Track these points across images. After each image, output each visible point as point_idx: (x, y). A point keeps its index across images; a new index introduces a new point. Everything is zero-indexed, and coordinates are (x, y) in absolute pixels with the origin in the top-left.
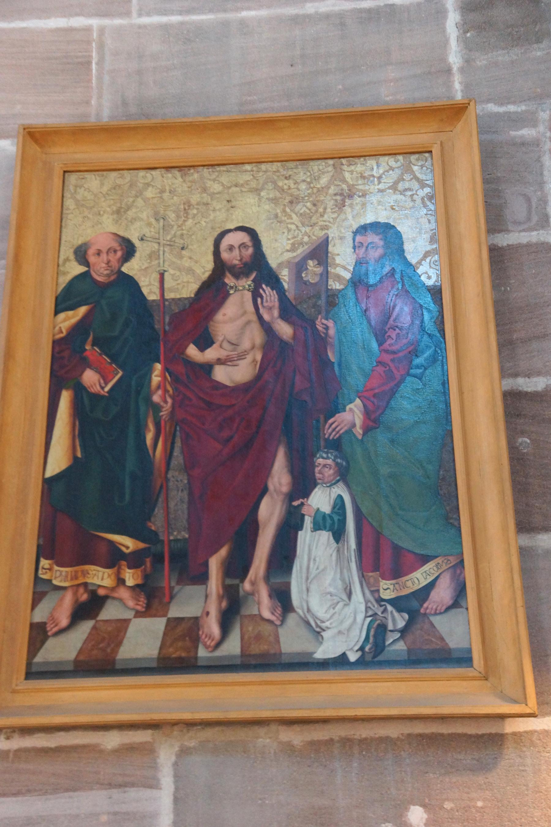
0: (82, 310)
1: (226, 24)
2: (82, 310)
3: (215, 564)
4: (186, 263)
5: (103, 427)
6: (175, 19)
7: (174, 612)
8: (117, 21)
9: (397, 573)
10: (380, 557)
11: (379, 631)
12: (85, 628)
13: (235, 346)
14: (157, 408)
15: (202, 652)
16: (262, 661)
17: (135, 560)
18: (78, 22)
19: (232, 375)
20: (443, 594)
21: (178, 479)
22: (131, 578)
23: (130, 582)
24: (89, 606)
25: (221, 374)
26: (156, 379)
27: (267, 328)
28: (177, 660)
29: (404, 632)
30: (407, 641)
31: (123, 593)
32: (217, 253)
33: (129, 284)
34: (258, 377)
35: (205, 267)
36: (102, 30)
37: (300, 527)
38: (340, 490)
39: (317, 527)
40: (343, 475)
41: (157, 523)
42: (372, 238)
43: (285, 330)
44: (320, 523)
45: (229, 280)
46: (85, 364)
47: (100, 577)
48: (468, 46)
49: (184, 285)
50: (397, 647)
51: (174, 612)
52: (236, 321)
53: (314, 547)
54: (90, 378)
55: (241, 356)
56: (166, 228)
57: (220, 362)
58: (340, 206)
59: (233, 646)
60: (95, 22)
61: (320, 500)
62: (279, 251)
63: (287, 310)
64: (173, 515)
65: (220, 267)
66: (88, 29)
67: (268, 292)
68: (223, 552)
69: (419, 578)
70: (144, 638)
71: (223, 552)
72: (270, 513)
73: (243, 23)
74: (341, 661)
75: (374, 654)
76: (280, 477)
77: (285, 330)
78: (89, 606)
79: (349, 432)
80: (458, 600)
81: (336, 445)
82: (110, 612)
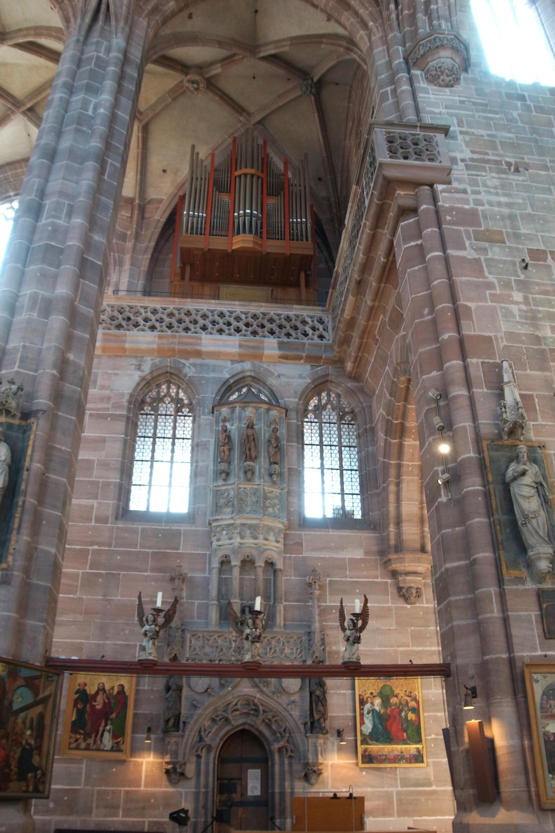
3: (93, 735)
5: (80, 713)
10: (115, 736)
11: (113, 747)
13: (99, 704)
16: (98, 750)
17: (83, 734)
19: (99, 707)
24: (77, 740)
28: (87, 748)
30: (116, 748)
33: (85, 691)
40: (112, 724)
43: (106, 701)
47: (78, 736)
50: (115, 749)
53: (106, 734)
54: (79, 706)
59: (94, 747)
60: (84, 641)
61: (108, 728)
62: (107, 687)
63: (107, 698)
64: (88, 727)
65: (99, 689)
69: (119, 740)
70: (83, 745)
72: (101, 729)
74: (107, 751)
75: (112, 750)
76: (103, 724)
77: (106, 701)
78: (77, 740)
80: (123, 743)
82: (79, 741)
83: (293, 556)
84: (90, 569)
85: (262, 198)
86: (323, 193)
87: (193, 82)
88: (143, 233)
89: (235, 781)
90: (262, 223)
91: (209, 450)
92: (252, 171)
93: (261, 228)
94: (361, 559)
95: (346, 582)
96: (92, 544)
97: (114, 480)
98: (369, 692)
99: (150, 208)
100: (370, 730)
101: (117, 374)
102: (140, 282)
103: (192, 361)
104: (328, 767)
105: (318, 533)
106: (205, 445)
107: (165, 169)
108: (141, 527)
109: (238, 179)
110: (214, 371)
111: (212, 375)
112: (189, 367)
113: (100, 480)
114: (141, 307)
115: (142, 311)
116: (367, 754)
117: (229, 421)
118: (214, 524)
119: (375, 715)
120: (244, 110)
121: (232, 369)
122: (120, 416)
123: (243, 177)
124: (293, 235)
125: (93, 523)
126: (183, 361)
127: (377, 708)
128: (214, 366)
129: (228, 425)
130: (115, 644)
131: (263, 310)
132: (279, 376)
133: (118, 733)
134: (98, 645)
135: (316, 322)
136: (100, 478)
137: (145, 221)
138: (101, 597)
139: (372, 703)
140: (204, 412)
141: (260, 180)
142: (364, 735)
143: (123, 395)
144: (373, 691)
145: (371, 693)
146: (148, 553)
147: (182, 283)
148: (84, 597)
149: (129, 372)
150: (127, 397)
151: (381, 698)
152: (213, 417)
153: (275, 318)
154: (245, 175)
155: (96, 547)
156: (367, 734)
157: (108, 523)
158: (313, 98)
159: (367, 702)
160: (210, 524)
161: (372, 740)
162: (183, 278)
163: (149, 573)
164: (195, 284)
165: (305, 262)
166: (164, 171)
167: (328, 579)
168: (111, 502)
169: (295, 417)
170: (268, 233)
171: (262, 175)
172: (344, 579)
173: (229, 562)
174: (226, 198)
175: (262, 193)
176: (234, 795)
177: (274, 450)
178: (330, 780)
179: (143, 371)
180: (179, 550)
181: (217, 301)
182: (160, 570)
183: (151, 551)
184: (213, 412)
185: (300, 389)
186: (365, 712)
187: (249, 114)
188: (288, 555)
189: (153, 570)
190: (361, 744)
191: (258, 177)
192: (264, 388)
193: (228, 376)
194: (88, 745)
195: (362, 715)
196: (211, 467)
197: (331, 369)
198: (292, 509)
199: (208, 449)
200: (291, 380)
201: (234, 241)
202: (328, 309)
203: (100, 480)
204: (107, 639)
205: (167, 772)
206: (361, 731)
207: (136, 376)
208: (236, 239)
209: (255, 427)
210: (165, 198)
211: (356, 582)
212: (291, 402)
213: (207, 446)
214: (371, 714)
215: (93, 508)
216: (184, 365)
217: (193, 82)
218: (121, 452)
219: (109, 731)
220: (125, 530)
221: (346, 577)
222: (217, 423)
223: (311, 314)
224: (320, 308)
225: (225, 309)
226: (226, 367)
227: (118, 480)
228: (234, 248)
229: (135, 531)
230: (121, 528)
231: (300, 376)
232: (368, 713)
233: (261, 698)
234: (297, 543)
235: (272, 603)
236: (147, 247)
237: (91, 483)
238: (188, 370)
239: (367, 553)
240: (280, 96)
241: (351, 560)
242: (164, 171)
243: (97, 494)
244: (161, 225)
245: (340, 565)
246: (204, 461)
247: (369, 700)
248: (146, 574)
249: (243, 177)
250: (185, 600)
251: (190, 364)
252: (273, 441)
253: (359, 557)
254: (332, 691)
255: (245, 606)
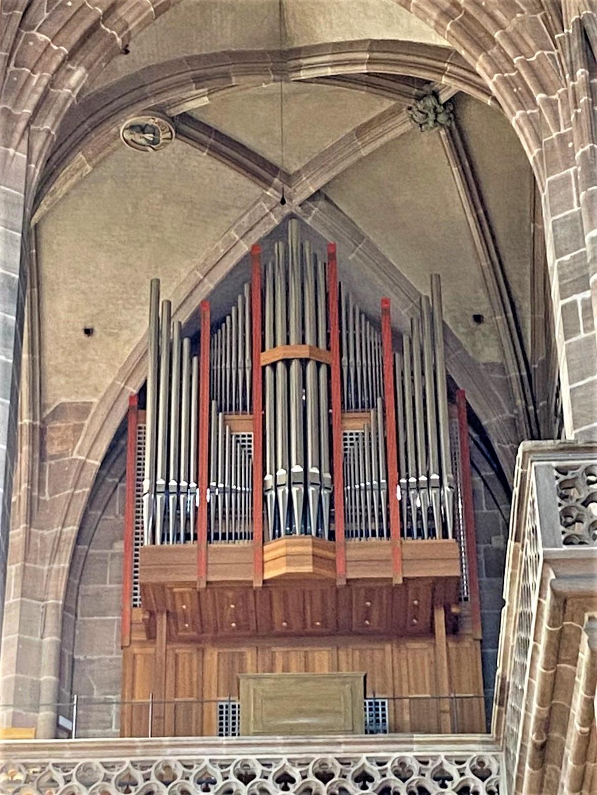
85: (330, 416)
86: (490, 354)
87: (142, 129)
88: (47, 497)
90: (332, 496)
92: (304, 352)
93: (332, 506)
99: (58, 430)
102: (47, 639)
107: (89, 326)
109: (268, 369)
114: (55, 765)
115: (59, 776)
120: (275, 170)
123: (280, 366)
124: (409, 518)
131: (342, 751)
135: (469, 775)
137: (48, 463)
141: (323, 370)
147: (150, 650)
153: (373, 770)
154: (287, 362)
158: (443, 133)
162: (151, 634)
164: (184, 651)
165: (444, 592)
166: (88, 332)
170: (347, 520)
171: (325, 357)
174: (244, 426)
175: (330, 406)
181: (234, 740)
187: (288, 178)
191: (318, 365)
201: (267, 557)
202: (498, 740)
208: (275, 549)
210: (95, 400)
217: (142, 129)
223: (457, 751)
224: (478, 737)
225: (253, 758)
228: (267, 576)
236: (59, 539)
240: (360, 131)
242: (88, 332)
244: (89, 476)
249: (280, 366)
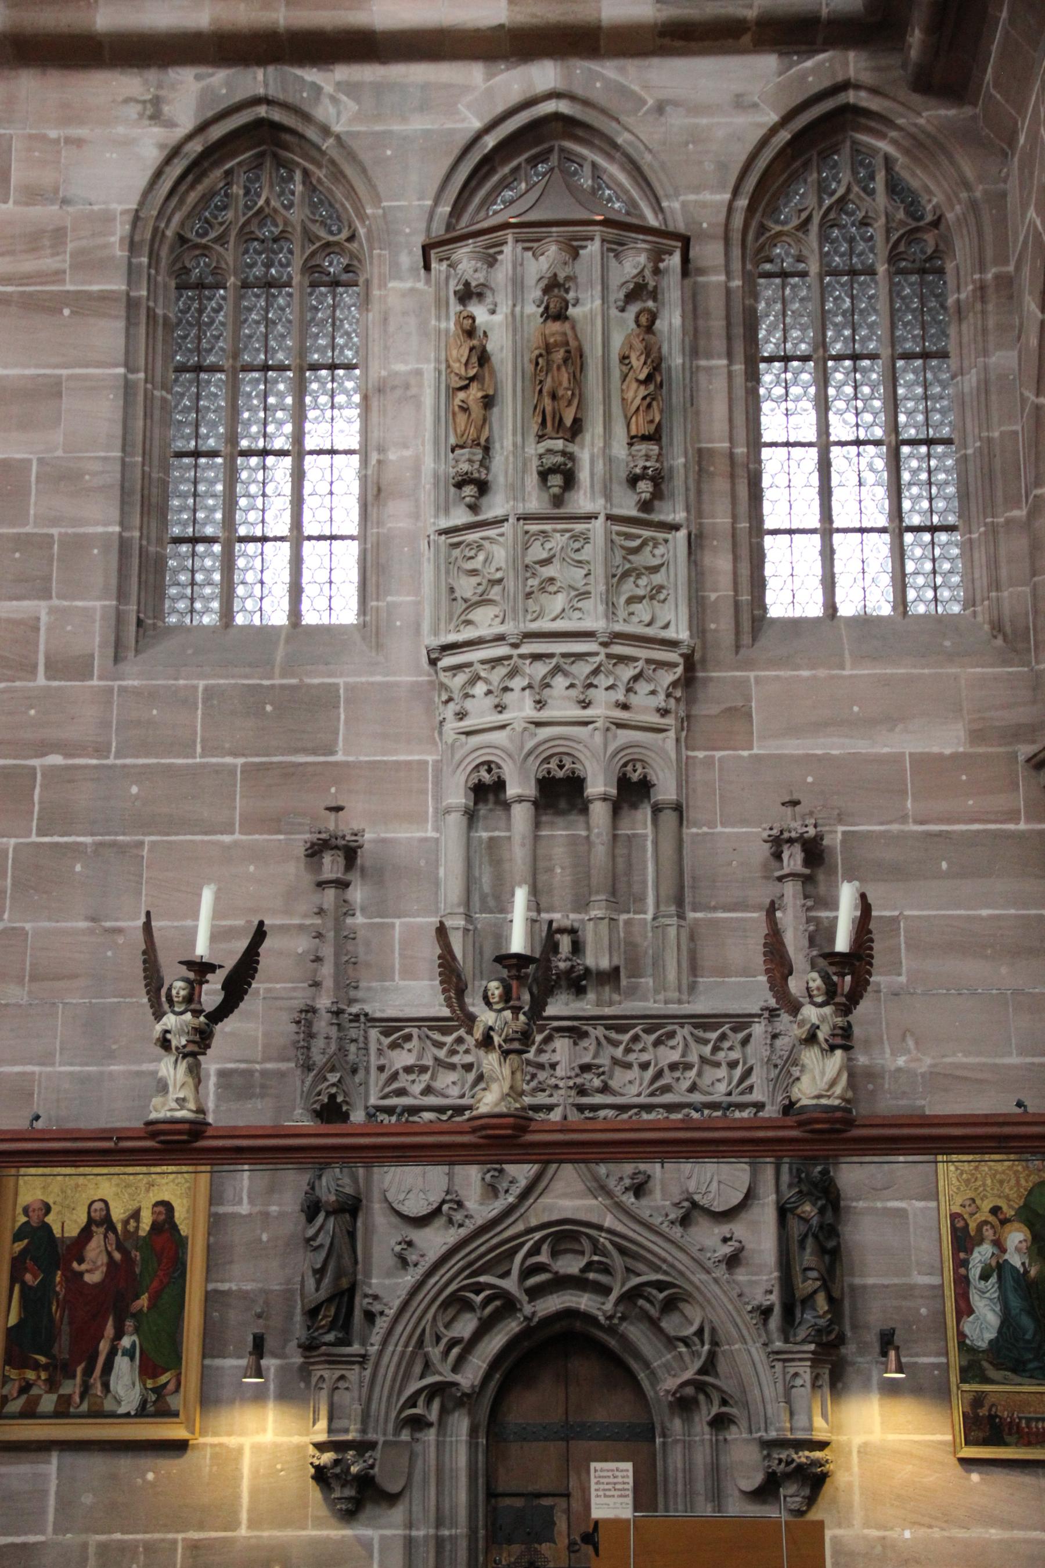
0: (26, 1241)
1: (102, 1073)
2: (26, 1241)
3: (79, 1370)
4: (74, 1217)
5: (34, 1302)
6: (77, 1068)
7: (62, 1391)
8: (49, 1069)
9: (154, 1376)
10: (148, 1369)
11: (144, 1403)
12: (24, 1397)
13: (93, 1266)
14: (58, 1294)
15: (72, 1410)
16: (97, 1414)
17: (45, 1368)
18: (29, 1068)
19: (93, 1278)
20: (171, 1387)
21: (65, 1328)
22: (43, 1376)
23: (43, 1378)
24: (26, 1388)
25: (88, 1278)
26: (58, 1279)
27: (109, 1254)
28: (62, 1412)
29: (155, 1402)
30: (154, 1406)
31: (40, 1383)
32: (89, 1213)
33: (47, 1228)
34: (103, 1281)
35: (83, 1219)
36: (40, 1074)
37: (116, 1354)
38: (135, 1338)
39: (123, 1355)
40: (137, 1330)
41: (55, 1351)
42: (161, 1209)
43: (117, 1256)
44: (125, 1353)
45: (94, 1228)
46: (26, 1270)
47: (31, 1375)
48: (219, 1098)
49: (73, 1231)
50: (151, 1408)
51: (62, 1391)
52: (96, 1250)
53: (122, 1363)
54: (28, 1277)
55: (97, 1268)
56: (66, 1198)
57: (87, 1271)
58: (148, 1190)
59: (85, 1407)
60: (36, 1069)
61: (126, 1342)
62: (118, 1213)
63: (120, 1247)
64: (62, 1347)
65: (90, 1221)
66: (33, 1073)
67: (111, 1235)
68: (83, 1365)
69: (163, 1379)
70: (48, 1403)
71: (83, 1365)
72: (104, 1347)
73: (111, 1073)
74: (127, 1415)
75: (142, 1412)
76: (109, 1330)
77: (117, 1256)
78: (26, 1388)
79: (141, 1310)
80: (177, 1390)
81: (134, 1316)
82: (35, 1391)
83: (718, 754)
84: (40, 834)
89: (546, 1502)
91: (418, 406)
94: (954, 756)
95: (902, 836)
96: (43, 748)
97: (100, 529)
98: (986, 1206)
100: (990, 1335)
101: (79, 142)
103: (342, 72)
104: (850, 1452)
105: (805, 673)
106: (407, 387)
108: (202, 684)
110: (424, 107)
111: (418, 124)
112: (334, 100)
113: (55, 531)
116: (983, 1412)
117: (480, 296)
118: (448, 661)
119: (1010, 1283)
121: (489, 92)
122: (104, 297)
125: (41, 680)
126: (311, 75)
127: (1016, 1260)
128: (425, 87)
129: (480, 312)
130: (139, 1074)
132: (660, 108)
133: (159, 1360)
134: (84, 1079)
136: (55, 522)
138: (83, 924)
139: (999, 1245)
140: (395, 265)
142: (972, 1350)
143: (107, 218)
144: (1001, 1203)
145: (995, 1210)
146: (231, 770)
148: (28, 926)
149: (121, 130)
150: (121, 229)
151: (1030, 1225)
152: (428, 282)
155: (56, 759)
156: (983, 1345)
157: (91, 677)
159: (981, 1241)
160: (433, 662)
161: (998, 1367)
163: (237, 836)
167: (841, 829)
168: (98, 604)
169: (720, 260)
172: (895, 827)
173: (500, 785)
176: (545, 1548)
177: (643, 391)
178: (857, 1498)
179: (171, 124)
180: (332, 753)
182: (273, 823)
183: (240, 761)
184: (427, 267)
185: (741, 153)
186: (975, 1273)
188: (700, 754)
189: (253, 823)
190: (963, 1380)
192: (611, 158)
193: (476, 124)
194: (65, 1401)
195: (962, 1283)
196: (428, 464)
197: (854, 64)
198: (713, 596)
199: (416, 401)
200: (704, 121)
203: (55, 531)
204: (111, 1056)
205: (321, 1475)
206: (961, 1335)
207: (149, 146)
209: (571, 311)
211: (940, 834)
212: (704, 205)
213: (413, 391)
214: (994, 1279)
215: (37, 629)
216: (317, 89)
218: (118, 430)
219: (130, 1353)
220: (151, 696)
221: (903, 819)
222: (441, 304)
226: (466, 89)
227: (117, 529)
229: (185, 700)
230: (137, 692)
231: (740, 103)
232: (985, 1277)
233: (620, 1228)
234: (731, 712)
235: (649, 916)
237: (22, 542)
238: (332, 110)
239: (976, 736)
241: (923, 762)
243: (48, 579)
245: (884, 780)
246: (405, 446)
247: (988, 1232)
248: (226, 838)
250: (360, 919)
251: (338, 84)
252: (636, 362)
253: (948, 751)
254: (861, 1204)
255: (561, 931)
